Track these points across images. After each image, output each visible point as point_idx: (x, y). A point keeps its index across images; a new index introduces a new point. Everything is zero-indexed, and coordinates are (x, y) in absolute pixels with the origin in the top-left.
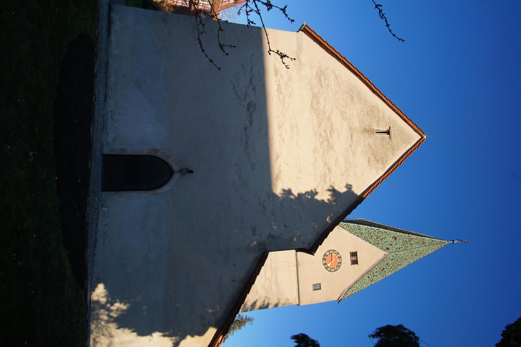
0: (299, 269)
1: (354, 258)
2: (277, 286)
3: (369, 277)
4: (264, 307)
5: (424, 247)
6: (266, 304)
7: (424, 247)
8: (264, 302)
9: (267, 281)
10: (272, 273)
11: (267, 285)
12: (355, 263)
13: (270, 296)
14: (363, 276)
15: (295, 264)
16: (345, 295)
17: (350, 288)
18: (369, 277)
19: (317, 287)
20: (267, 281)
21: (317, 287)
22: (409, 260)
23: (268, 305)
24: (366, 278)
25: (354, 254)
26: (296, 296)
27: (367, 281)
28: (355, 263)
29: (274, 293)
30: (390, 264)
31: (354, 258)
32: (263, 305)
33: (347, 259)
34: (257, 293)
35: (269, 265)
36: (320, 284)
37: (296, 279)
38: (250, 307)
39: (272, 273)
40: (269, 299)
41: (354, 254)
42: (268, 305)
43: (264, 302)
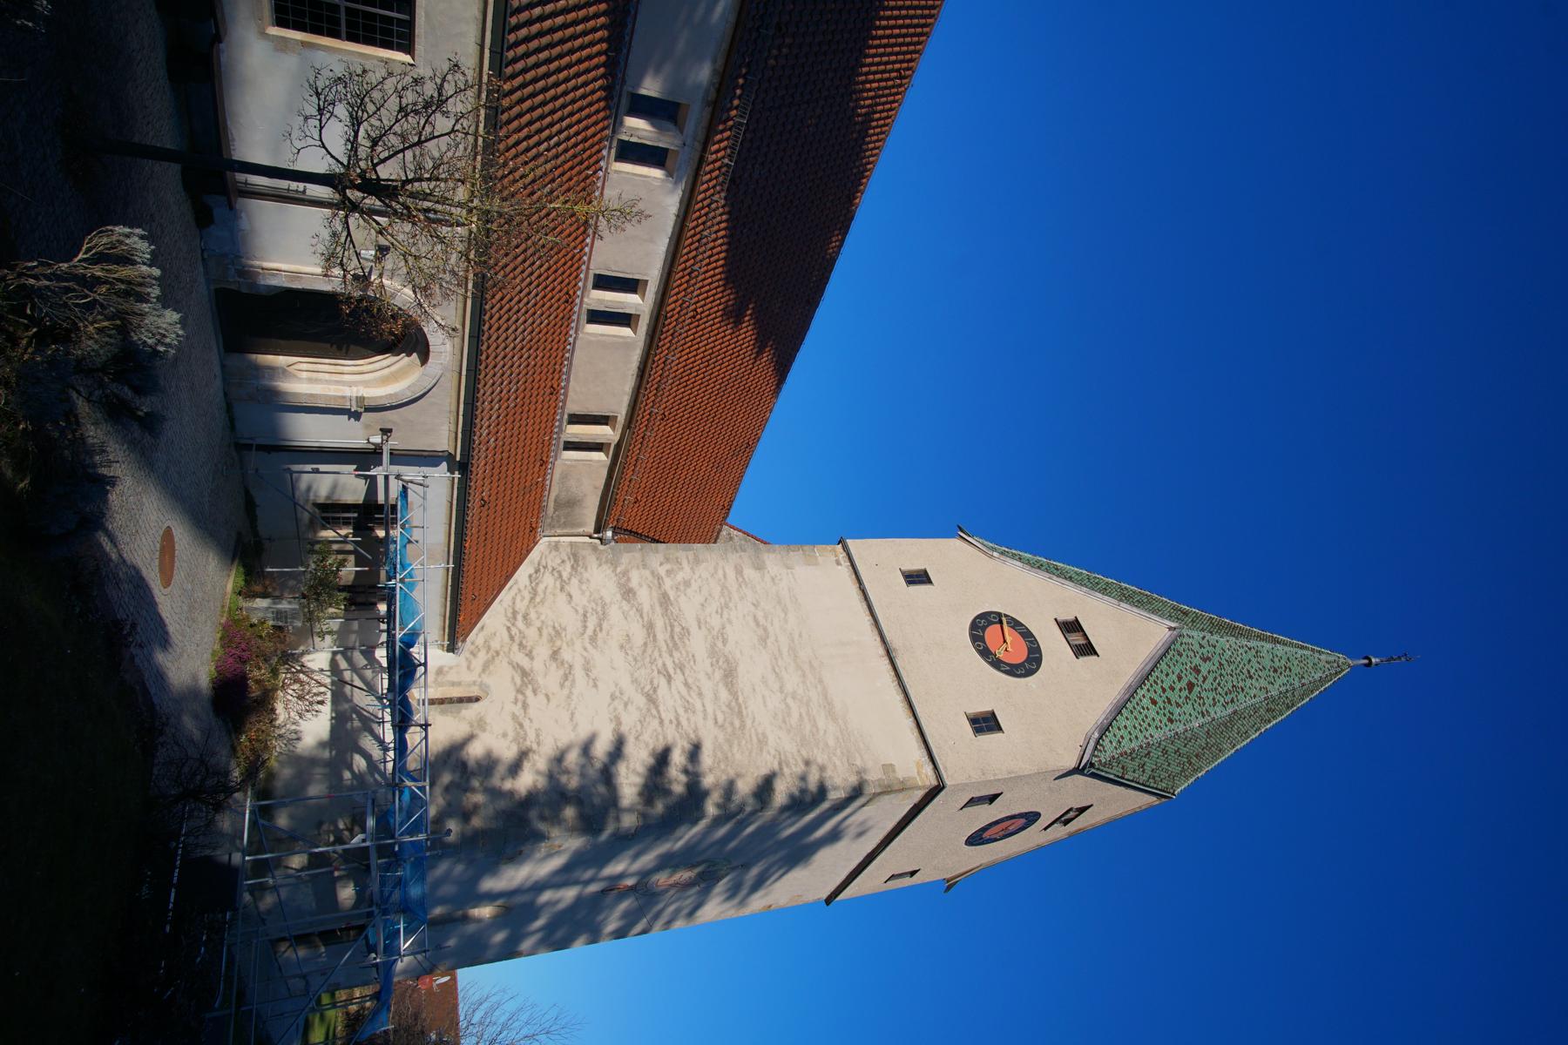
0: (899, 663)
1: (1077, 639)
2: (835, 720)
3: (1154, 702)
4: (808, 799)
5: (1284, 669)
6: (812, 785)
7: (1284, 669)
8: (803, 778)
9: (789, 700)
10: (804, 675)
11: (795, 715)
12: (1086, 649)
13: (821, 758)
14: (1131, 693)
15: (881, 651)
16: (1095, 748)
17: (1105, 729)
18: (1154, 702)
19: (985, 723)
20: (789, 700)
21: (985, 723)
22: (1263, 683)
23: (822, 791)
24: (1146, 702)
25: (1071, 627)
26: (919, 754)
27: (1152, 714)
28: (1086, 649)
29: (831, 743)
30: (1204, 672)
31: (1077, 639)
32: (803, 791)
33: (1054, 645)
34: (762, 741)
35: (785, 650)
36: (993, 714)
37: (899, 697)
38: (751, 801)
39: (804, 675)
40: (822, 769)
41: (1071, 627)
42: (822, 791)
43: (803, 778)
